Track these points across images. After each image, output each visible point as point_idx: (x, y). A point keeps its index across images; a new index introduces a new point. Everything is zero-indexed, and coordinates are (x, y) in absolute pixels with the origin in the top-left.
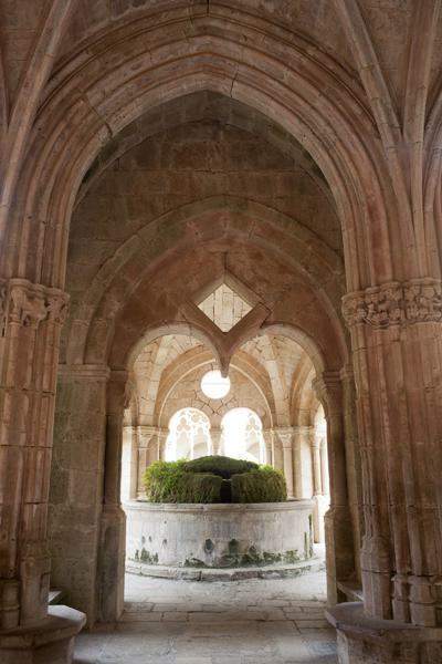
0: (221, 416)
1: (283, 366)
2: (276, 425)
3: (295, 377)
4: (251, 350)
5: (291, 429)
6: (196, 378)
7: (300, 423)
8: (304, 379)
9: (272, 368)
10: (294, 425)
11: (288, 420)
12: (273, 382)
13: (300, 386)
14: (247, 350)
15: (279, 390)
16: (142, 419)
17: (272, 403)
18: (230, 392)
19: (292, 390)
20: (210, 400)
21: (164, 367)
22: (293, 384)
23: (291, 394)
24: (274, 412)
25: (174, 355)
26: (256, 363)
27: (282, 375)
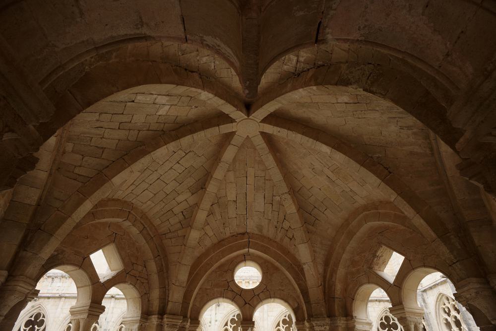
0: (253, 308)
1: (314, 251)
2: (311, 317)
3: (326, 263)
4: (282, 240)
5: (328, 321)
6: (231, 268)
7: (337, 314)
8: (336, 265)
9: (303, 253)
10: (331, 315)
11: (323, 310)
12: (306, 267)
13: (334, 272)
14: (278, 240)
15: (312, 275)
16: (170, 306)
17: (305, 292)
18: (261, 283)
19: (324, 277)
20: (243, 290)
21: (197, 254)
22: (325, 271)
23: (324, 281)
24: (308, 302)
25: (208, 243)
26: (287, 252)
27: (314, 260)
